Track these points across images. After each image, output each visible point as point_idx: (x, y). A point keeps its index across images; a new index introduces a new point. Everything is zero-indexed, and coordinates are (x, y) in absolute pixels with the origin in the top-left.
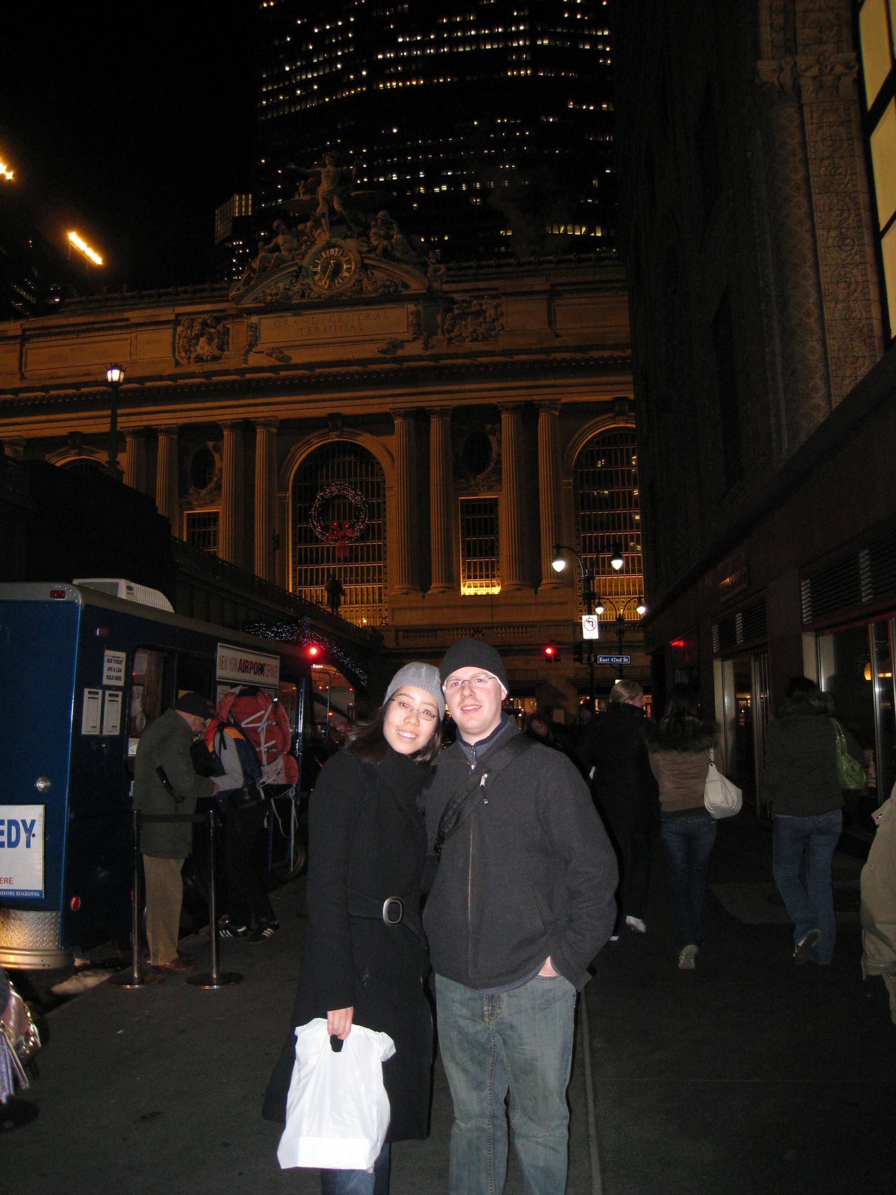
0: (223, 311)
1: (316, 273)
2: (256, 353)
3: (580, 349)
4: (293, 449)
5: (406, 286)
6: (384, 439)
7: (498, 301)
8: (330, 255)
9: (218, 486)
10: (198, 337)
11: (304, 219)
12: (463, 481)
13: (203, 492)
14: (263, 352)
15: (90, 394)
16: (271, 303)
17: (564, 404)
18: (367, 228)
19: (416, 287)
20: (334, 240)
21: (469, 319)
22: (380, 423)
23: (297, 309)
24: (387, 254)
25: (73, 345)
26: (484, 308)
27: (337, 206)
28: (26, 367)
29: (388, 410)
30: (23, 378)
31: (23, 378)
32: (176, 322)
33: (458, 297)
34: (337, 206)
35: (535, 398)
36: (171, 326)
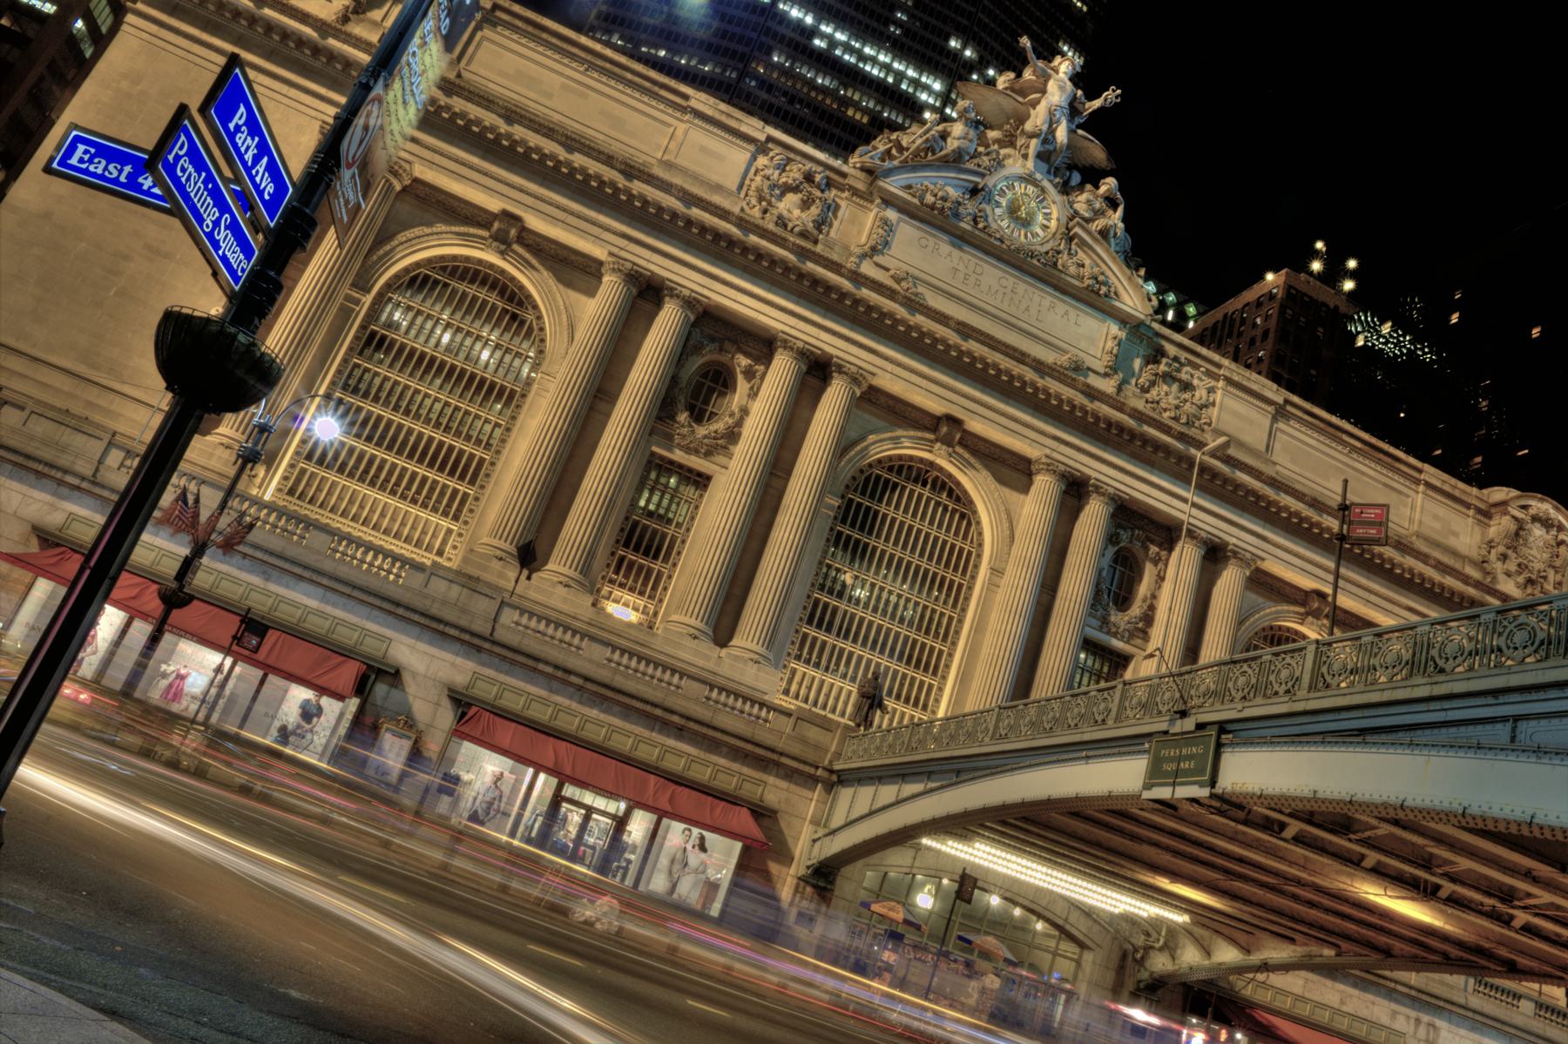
0: (844, 175)
2: (877, 265)
4: (872, 438)
6: (1007, 492)
7: (1213, 383)
10: (787, 189)
13: (701, 431)
14: (887, 270)
16: (932, 207)
20: (1038, 176)
21: (1175, 387)
22: (1013, 470)
23: (962, 239)
25: (568, 77)
26: (1195, 382)
27: (1061, 134)
28: (468, 63)
32: (762, 148)
33: (1171, 350)
34: (1061, 134)
36: (752, 148)
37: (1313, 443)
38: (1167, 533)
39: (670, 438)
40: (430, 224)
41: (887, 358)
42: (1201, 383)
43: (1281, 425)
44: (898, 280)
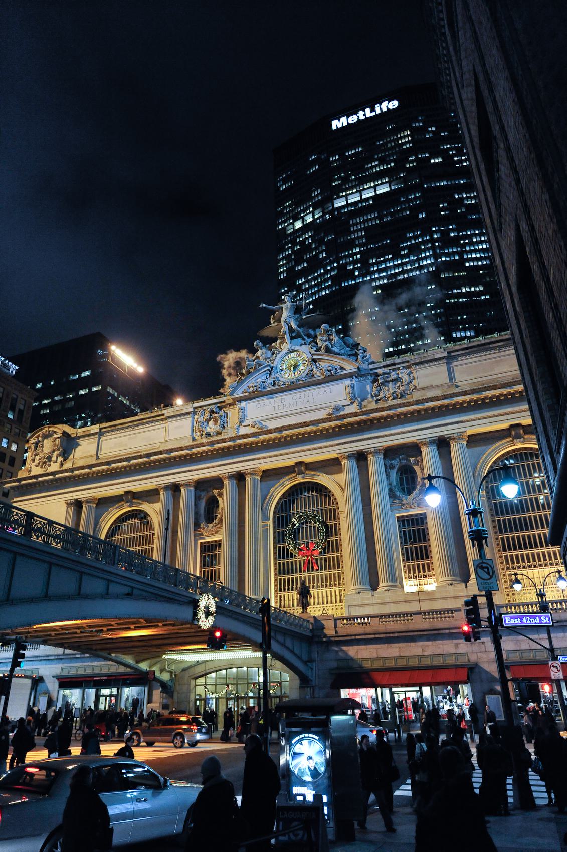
0: (223, 402)
1: (282, 370)
3: (473, 392)
5: (342, 369)
8: (291, 357)
9: (221, 521)
10: (208, 421)
11: (275, 340)
12: (397, 501)
13: (210, 526)
15: (137, 464)
16: (253, 392)
17: (469, 436)
18: (316, 337)
19: (350, 368)
24: (328, 350)
29: (336, 456)
30: (98, 458)
31: (98, 458)
32: (195, 413)
33: (380, 371)
34: (294, 326)
35: (446, 432)
36: (191, 416)
37: (477, 359)
38: (414, 449)
39: (202, 534)
40: (107, 510)
41: (265, 458)
42: (404, 375)
43: (454, 364)
44: (253, 427)
